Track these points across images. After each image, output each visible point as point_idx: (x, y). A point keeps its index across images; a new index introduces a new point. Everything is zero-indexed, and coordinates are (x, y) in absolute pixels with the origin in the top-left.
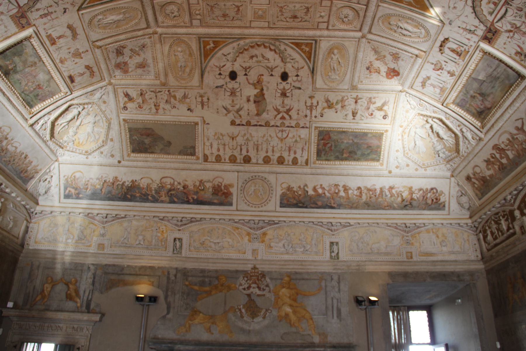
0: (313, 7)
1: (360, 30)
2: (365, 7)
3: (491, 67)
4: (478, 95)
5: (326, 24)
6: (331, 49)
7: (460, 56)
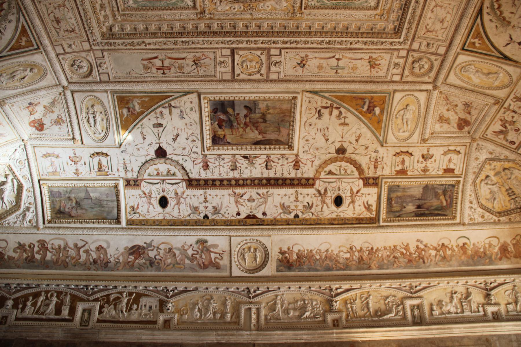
0: (78, 35)
1: (69, 83)
2: (99, 81)
3: (107, 197)
4: (74, 201)
5: (62, 51)
6: (35, 65)
7: (99, 171)
